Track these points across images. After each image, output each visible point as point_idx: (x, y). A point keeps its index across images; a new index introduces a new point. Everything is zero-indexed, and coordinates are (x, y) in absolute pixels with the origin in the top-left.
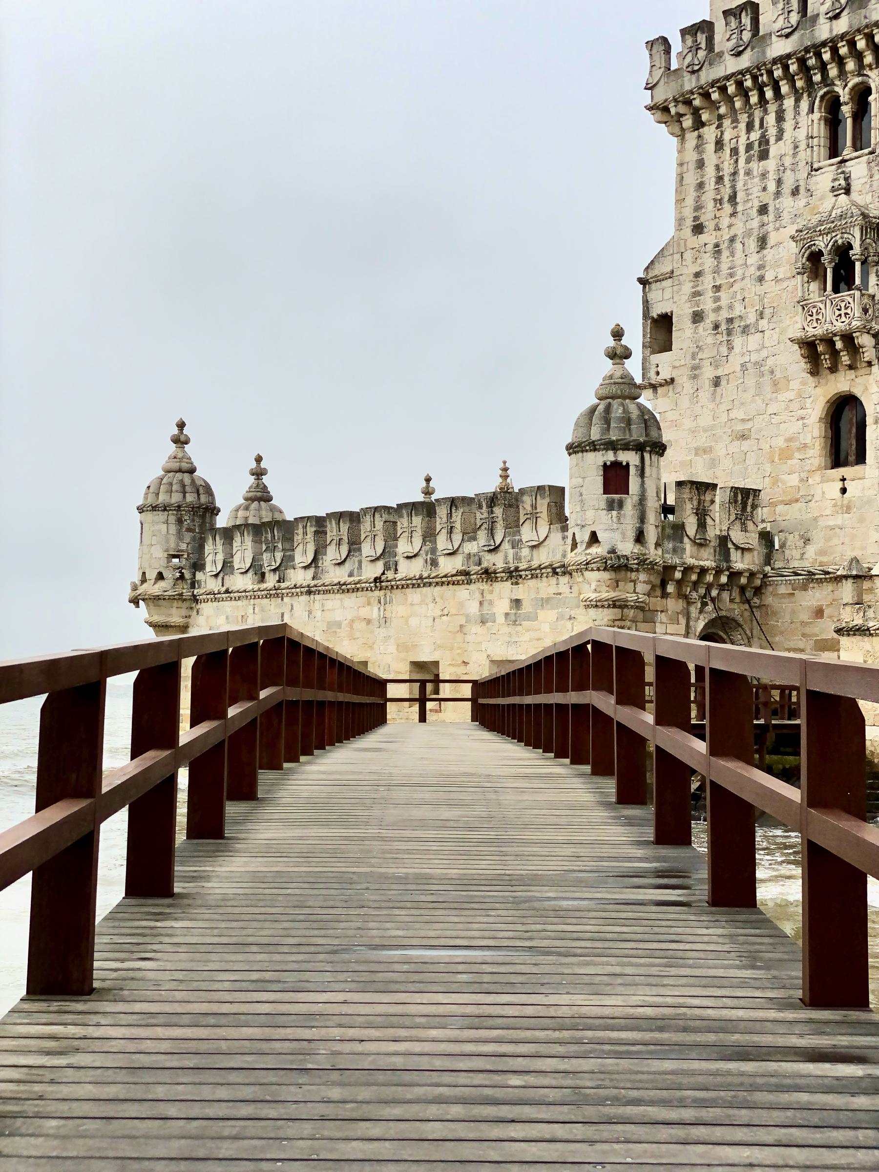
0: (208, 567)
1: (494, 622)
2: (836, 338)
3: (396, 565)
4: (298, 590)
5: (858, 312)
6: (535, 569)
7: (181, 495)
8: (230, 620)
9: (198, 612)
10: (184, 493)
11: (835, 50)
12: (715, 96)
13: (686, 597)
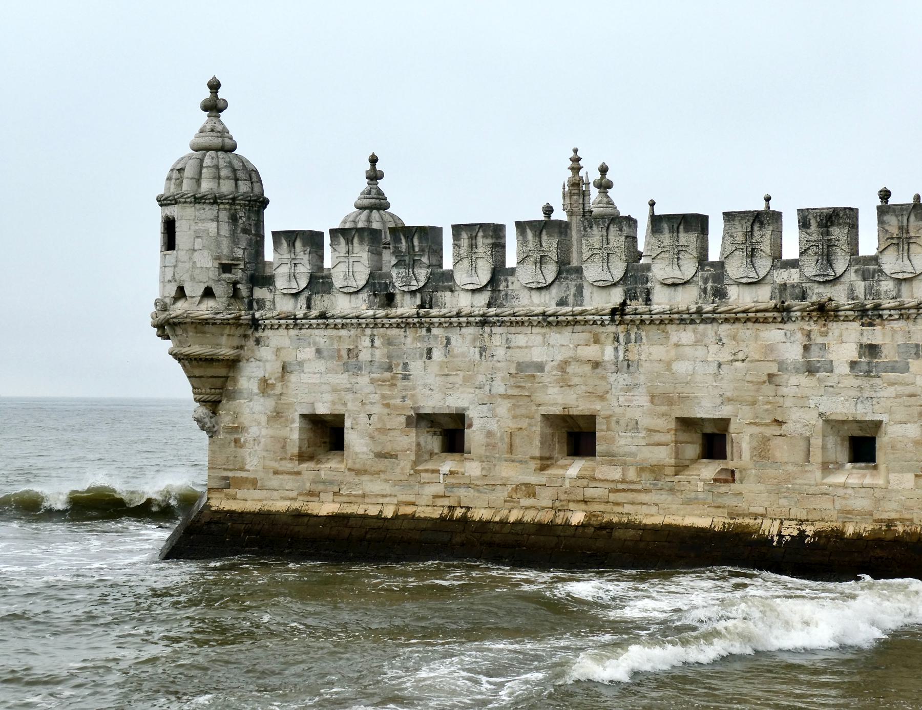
0: (281, 283)
1: (832, 371)
3: (648, 292)
4: (464, 319)
6: (909, 309)
7: (232, 182)
8: (325, 354)
9: (258, 341)
10: (237, 180)
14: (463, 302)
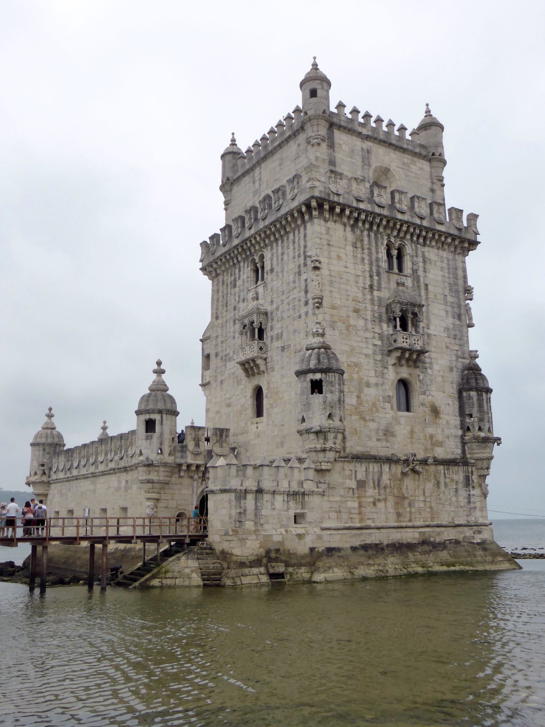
2: (250, 361)
5: (256, 349)
7: (45, 439)
10: (47, 437)
11: (251, 241)
12: (219, 263)
13: (192, 477)
14: (75, 472)
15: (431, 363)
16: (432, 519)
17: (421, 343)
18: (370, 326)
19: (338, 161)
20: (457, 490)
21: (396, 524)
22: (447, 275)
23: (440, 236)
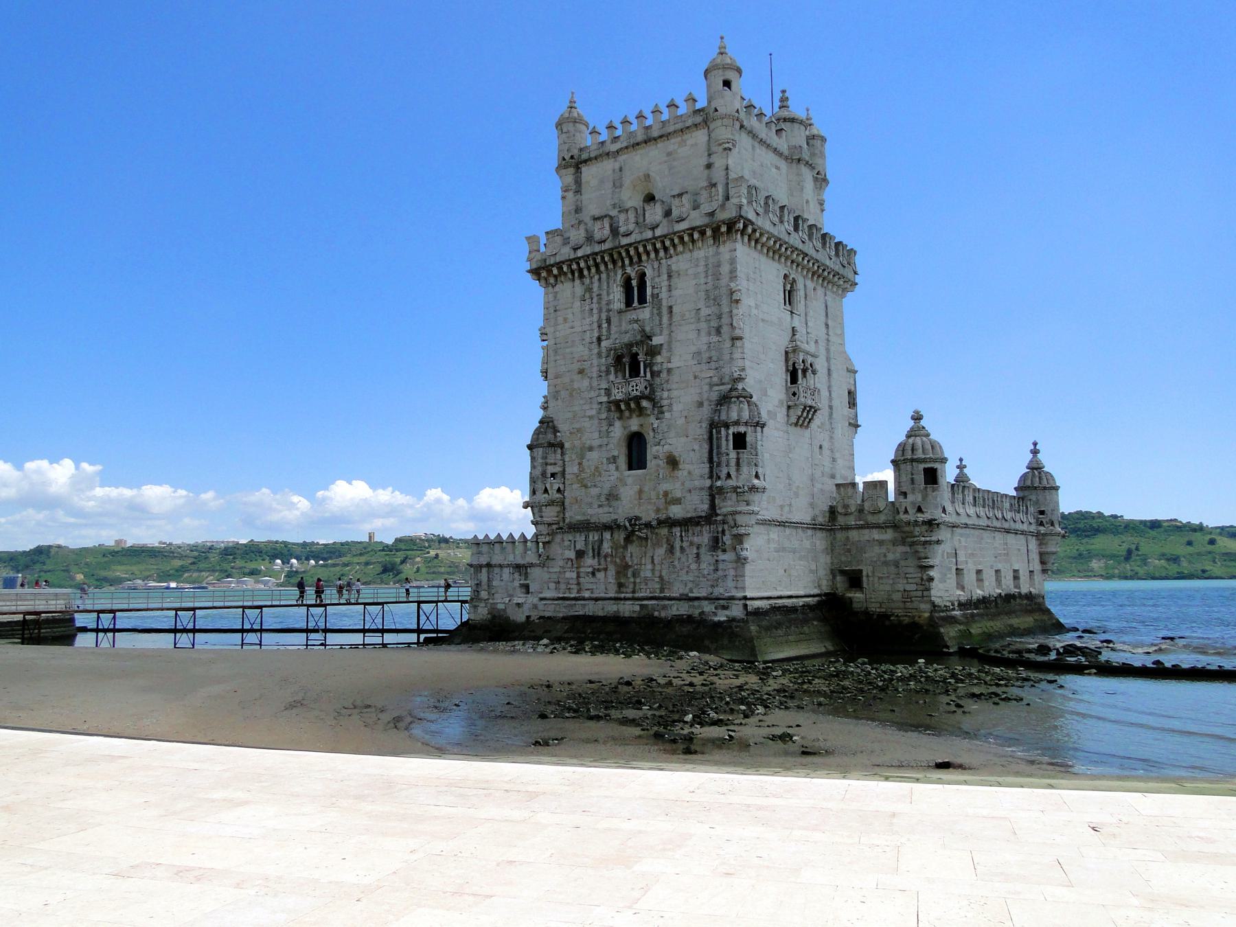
15: (670, 405)
16: (662, 590)
17: (641, 387)
18: (595, 383)
19: (584, 203)
20: (698, 555)
21: (612, 595)
22: (703, 281)
23: (681, 238)
